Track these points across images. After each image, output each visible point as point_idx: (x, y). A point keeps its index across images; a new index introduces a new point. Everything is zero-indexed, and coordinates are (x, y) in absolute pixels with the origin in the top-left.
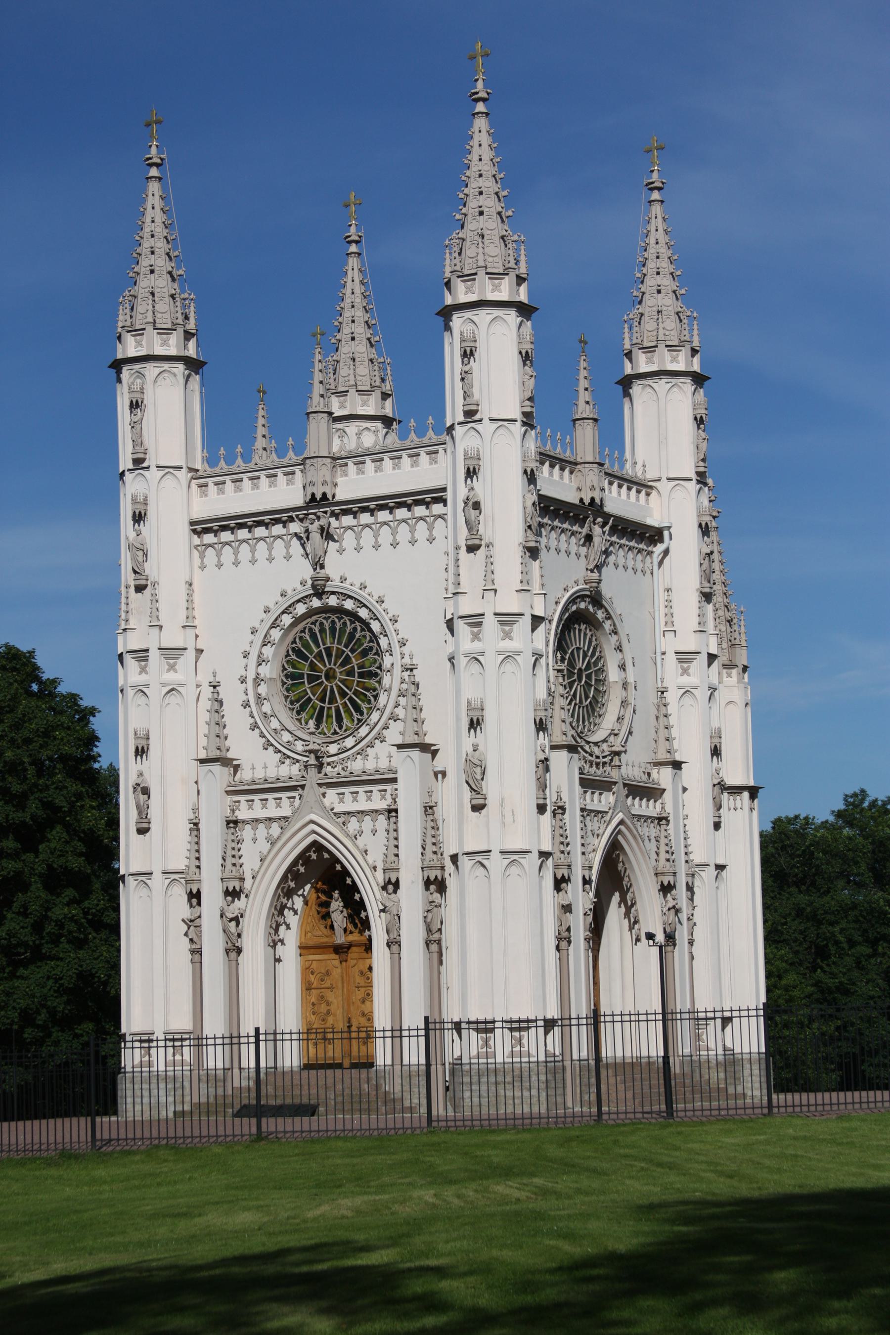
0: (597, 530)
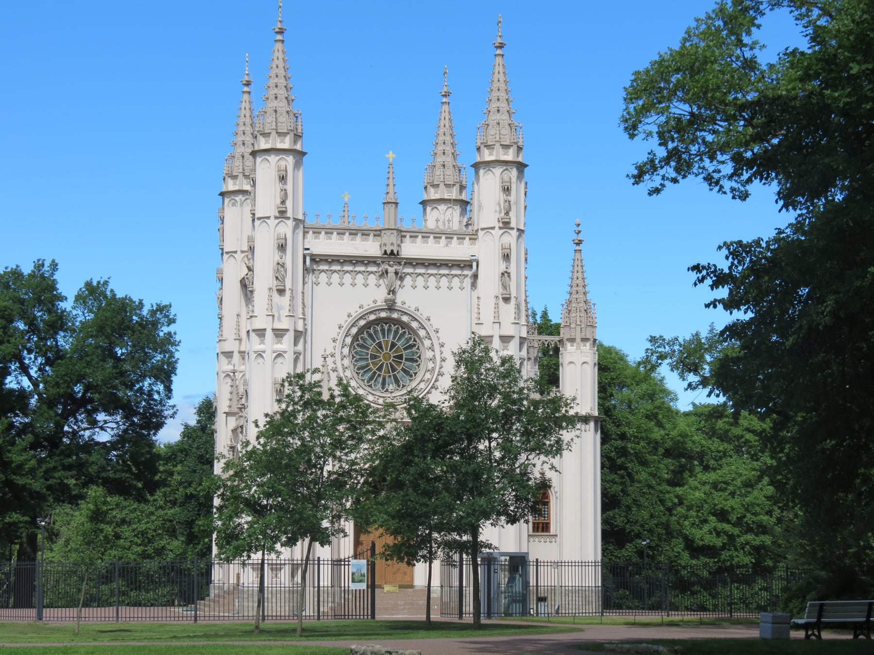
0: (391, 270)
